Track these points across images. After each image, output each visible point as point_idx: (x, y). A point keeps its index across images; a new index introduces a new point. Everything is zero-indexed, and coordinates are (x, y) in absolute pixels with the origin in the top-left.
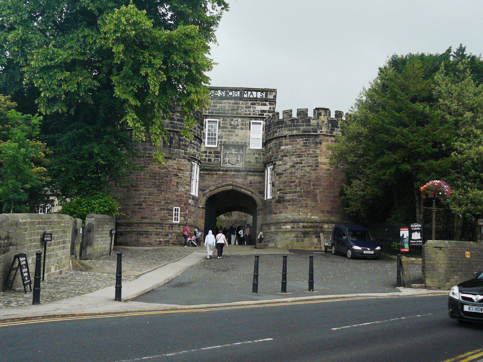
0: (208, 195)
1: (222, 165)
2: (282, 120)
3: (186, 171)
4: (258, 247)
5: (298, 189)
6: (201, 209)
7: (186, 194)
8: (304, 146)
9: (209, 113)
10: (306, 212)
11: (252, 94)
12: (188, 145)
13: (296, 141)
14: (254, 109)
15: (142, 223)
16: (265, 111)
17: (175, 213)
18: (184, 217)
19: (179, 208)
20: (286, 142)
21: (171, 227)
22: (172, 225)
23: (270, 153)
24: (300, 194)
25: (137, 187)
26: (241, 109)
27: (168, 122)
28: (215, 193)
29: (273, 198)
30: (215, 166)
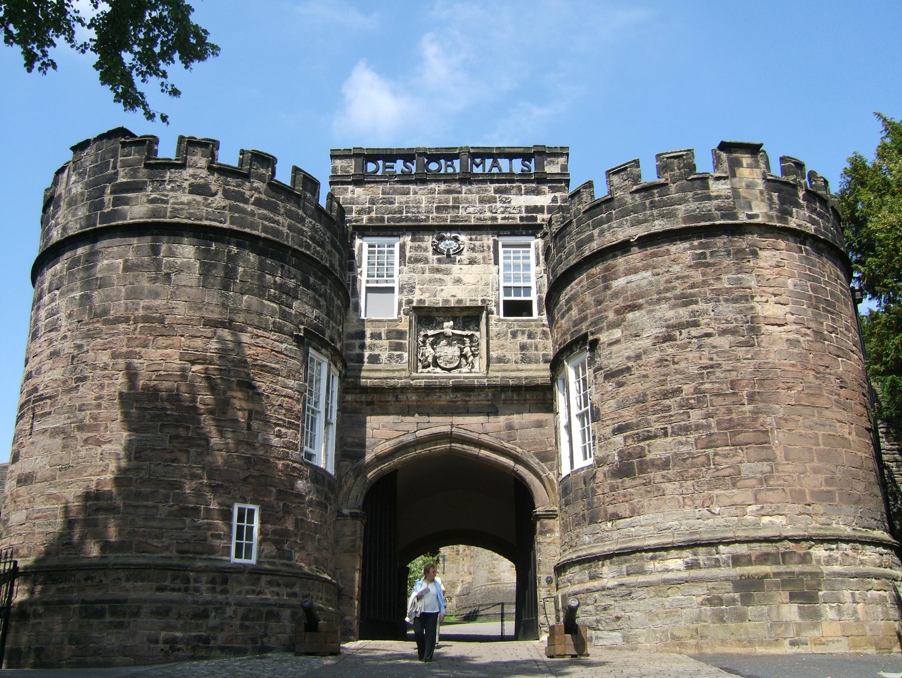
2: (609, 197)
5: (696, 416)
9: (370, 219)
11: (495, 164)
14: (507, 205)
16: (539, 209)
17: (240, 529)
18: (277, 543)
20: (627, 262)
23: (574, 312)
24: (703, 433)
26: (466, 205)
27: (224, 204)
29: (599, 462)
30: (390, 374)
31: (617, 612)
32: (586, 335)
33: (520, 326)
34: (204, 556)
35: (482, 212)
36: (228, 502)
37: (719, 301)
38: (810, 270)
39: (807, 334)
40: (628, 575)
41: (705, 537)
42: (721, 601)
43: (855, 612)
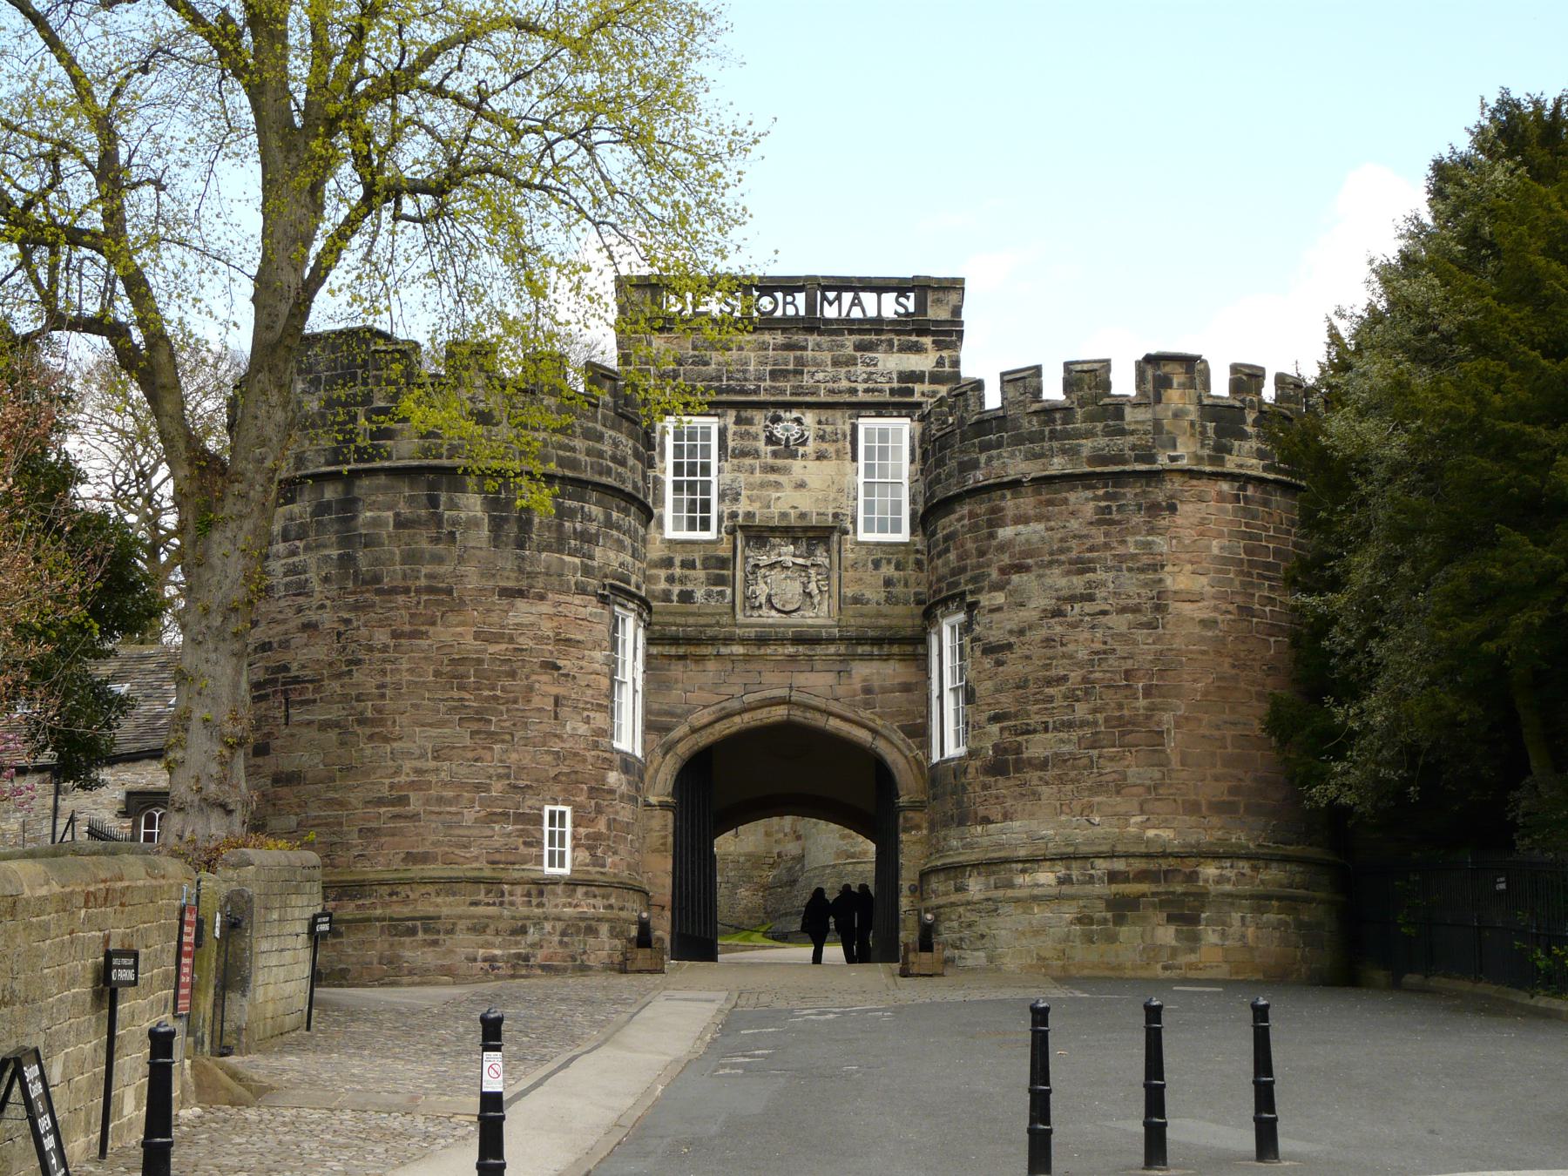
0: (683, 749)
1: (740, 617)
2: (1001, 413)
3: (590, 646)
4: (914, 970)
5: (1081, 711)
6: (658, 812)
7: (596, 746)
8: (1100, 522)
10: (1118, 809)
12: (597, 535)
13: (1065, 501)
15: (410, 882)
16: (916, 377)
17: (552, 834)
18: (591, 849)
19: (568, 810)
20: (1018, 507)
21: (534, 892)
22: (541, 886)
23: (952, 556)
24: (1088, 731)
25: (380, 722)
26: (814, 369)
28: (712, 738)
29: (972, 754)
31: (982, 929)
32: (963, 594)
33: (885, 553)
34: (517, 867)
35: (835, 380)
36: (538, 805)
37: (1121, 570)
38: (1247, 525)
39: (1229, 612)
40: (996, 888)
41: (1084, 849)
42: (1091, 921)
43: (1243, 936)
